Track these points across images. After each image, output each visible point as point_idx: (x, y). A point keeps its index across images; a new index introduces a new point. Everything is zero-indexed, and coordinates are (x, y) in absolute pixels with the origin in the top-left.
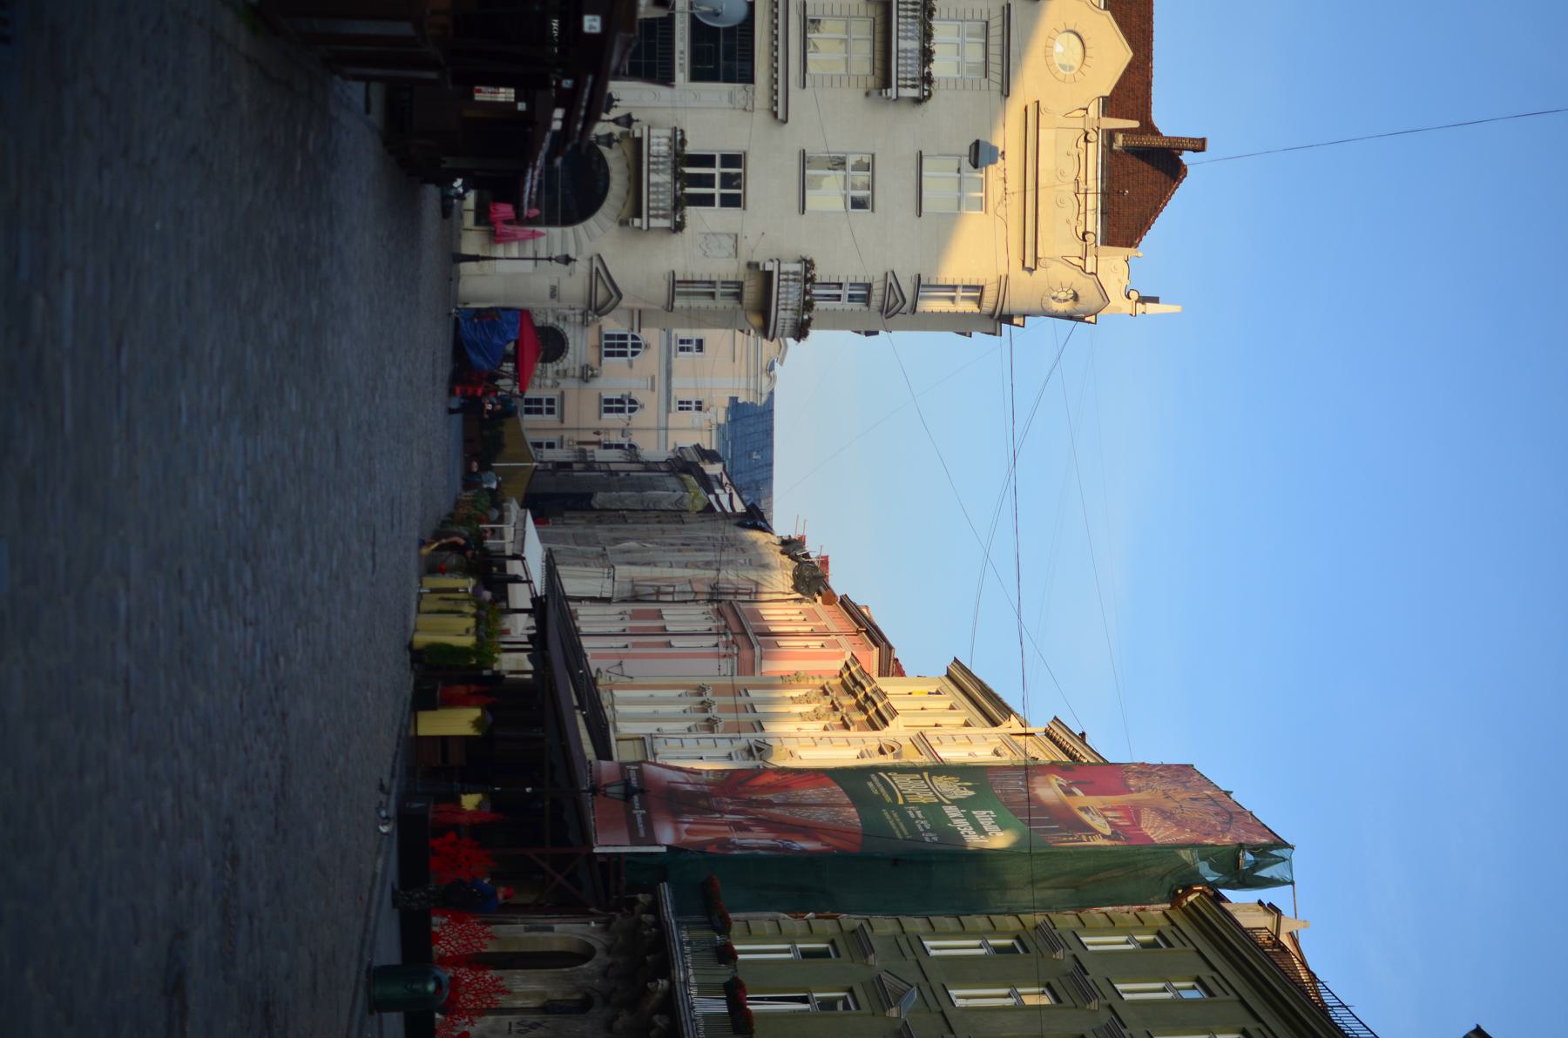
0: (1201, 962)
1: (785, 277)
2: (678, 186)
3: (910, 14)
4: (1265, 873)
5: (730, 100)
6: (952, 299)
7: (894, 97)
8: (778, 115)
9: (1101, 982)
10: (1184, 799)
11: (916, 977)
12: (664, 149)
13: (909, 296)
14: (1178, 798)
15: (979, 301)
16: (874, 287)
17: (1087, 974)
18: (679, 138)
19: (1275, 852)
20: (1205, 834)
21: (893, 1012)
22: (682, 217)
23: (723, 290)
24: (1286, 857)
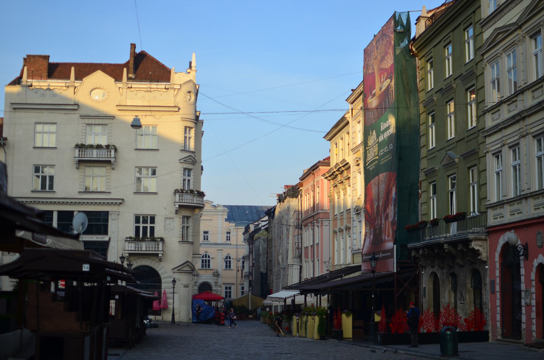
0: (438, 46)
2: (147, 240)
3: (83, 153)
4: (405, 22)
5: (115, 220)
6: (190, 138)
7: (114, 159)
8: (121, 202)
9: (446, 83)
10: (377, 52)
11: (443, 152)
12: (133, 245)
13: (188, 154)
14: (377, 55)
15: (190, 128)
16: (185, 167)
17: (442, 88)
18: (129, 239)
19: (397, 18)
20: (390, 44)
21: (457, 160)
22: (158, 238)
24: (399, 14)
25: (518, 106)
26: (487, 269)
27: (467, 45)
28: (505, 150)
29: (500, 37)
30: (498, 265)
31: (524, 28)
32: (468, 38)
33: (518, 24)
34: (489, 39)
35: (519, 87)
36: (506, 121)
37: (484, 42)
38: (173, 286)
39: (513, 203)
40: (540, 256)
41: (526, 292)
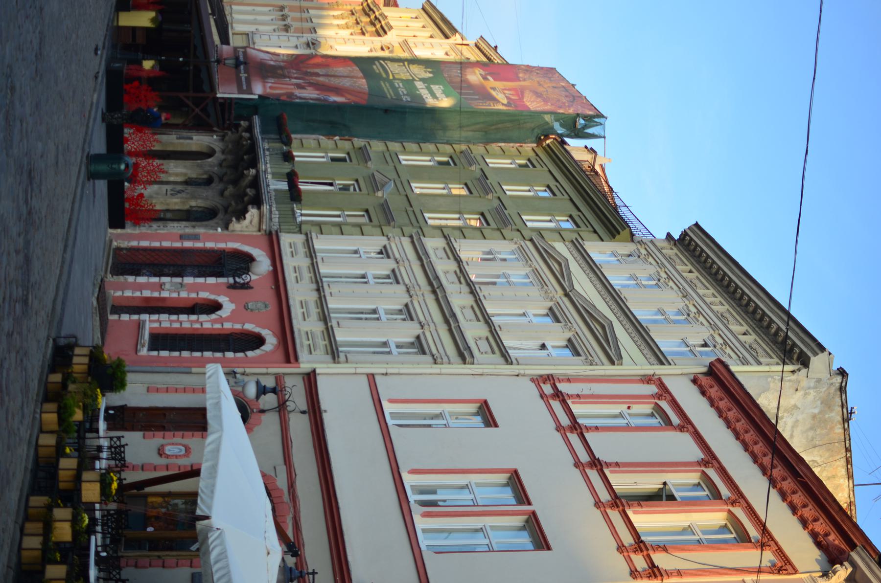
4: (590, 131)
11: (393, 175)
14: (546, 86)
17: (487, 179)
19: (596, 120)
20: (559, 107)
21: (380, 194)
24: (602, 122)
25: (453, 285)
26: (217, 230)
27: (548, 218)
28: (391, 264)
29: (555, 267)
30: (222, 245)
31: (565, 300)
32: (558, 221)
35: (480, 288)
37: (550, 243)
39: (306, 247)
40: (232, 306)
41: (181, 284)
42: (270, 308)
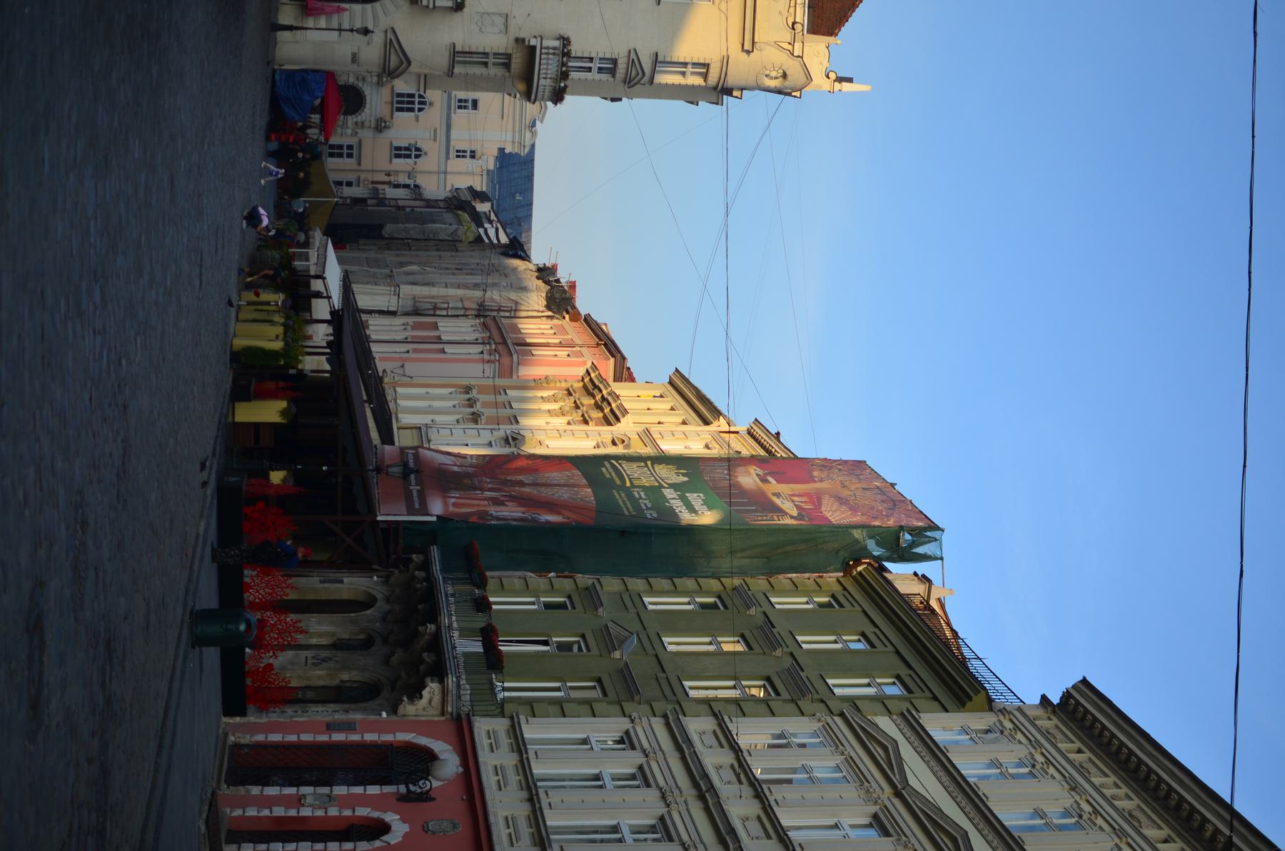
0: (866, 620)
1: (546, 51)
4: (920, 550)
6: (683, 74)
9: (785, 635)
10: (857, 488)
11: (635, 626)
16: (619, 61)
17: (774, 627)
19: (928, 534)
20: (873, 517)
21: (617, 655)
23: (494, 60)
24: (938, 537)
26: (380, 715)
27: (865, 681)
28: (637, 758)
30: (388, 737)
31: (896, 802)
32: (880, 684)
33: (903, 789)
34: (875, 727)
35: (769, 788)
36: (697, 762)
37: (869, 717)
38: (355, 28)
39: (512, 736)
40: (406, 828)
41: (329, 796)
42: (460, 829)
